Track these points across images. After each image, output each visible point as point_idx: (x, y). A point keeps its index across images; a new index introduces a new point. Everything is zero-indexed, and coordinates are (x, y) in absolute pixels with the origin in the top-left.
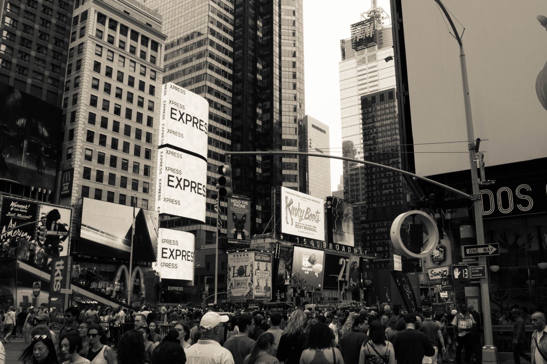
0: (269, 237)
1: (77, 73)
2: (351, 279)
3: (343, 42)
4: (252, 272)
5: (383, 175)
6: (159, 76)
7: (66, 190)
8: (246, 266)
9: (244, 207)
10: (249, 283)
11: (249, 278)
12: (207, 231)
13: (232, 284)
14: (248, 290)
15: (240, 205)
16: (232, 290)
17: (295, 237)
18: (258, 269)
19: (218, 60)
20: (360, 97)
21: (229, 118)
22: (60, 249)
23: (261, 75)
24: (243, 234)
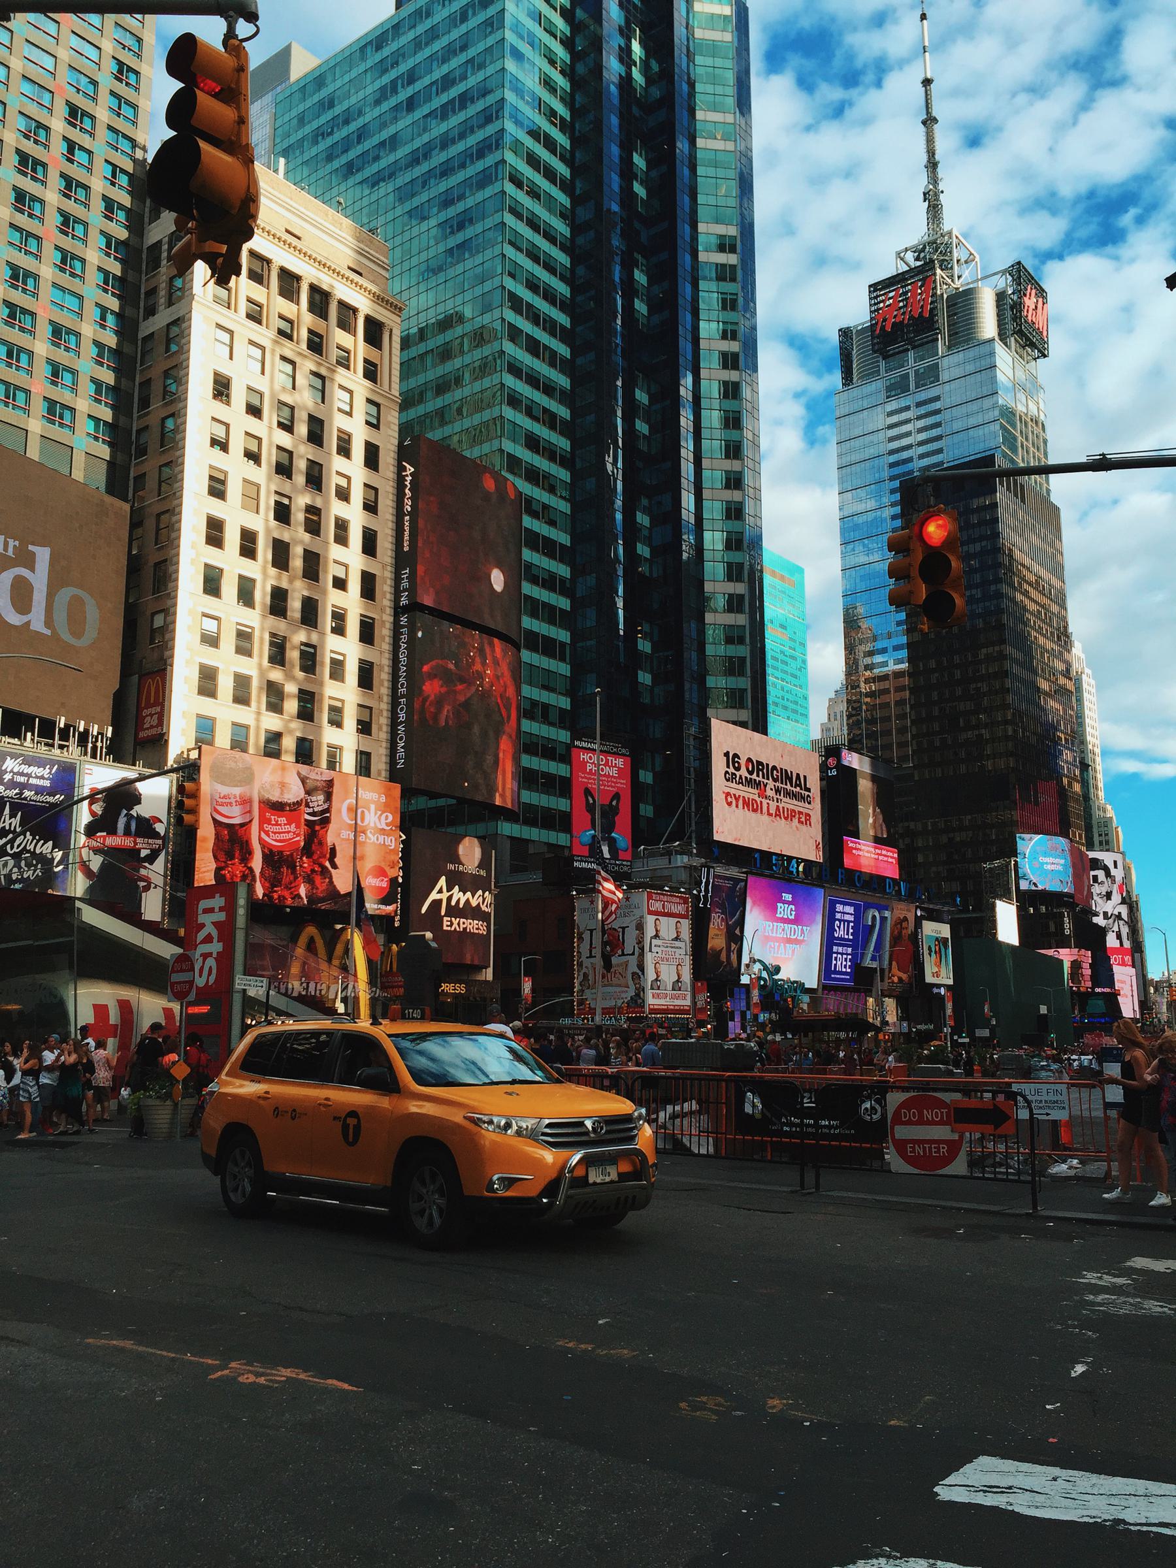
0: (677, 853)
1: (166, 405)
2: (894, 963)
3: (845, 333)
4: (639, 942)
5: (959, 692)
6: (390, 419)
7: (152, 727)
8: (623, 928)
9: (614, 772)
10: (634, 974)
11: (633, 961)
12: (512, 838)
13: (586, 976)
14: (631, 992)
15: (602, 768)
16: (588, 994)
17: (750, 851)
18: (657, 936)
19: (533, 380)
20: (897, 484)
21: (564, 539)
22: (142, 884)
23: (647, 421)
24: (612, 844)
